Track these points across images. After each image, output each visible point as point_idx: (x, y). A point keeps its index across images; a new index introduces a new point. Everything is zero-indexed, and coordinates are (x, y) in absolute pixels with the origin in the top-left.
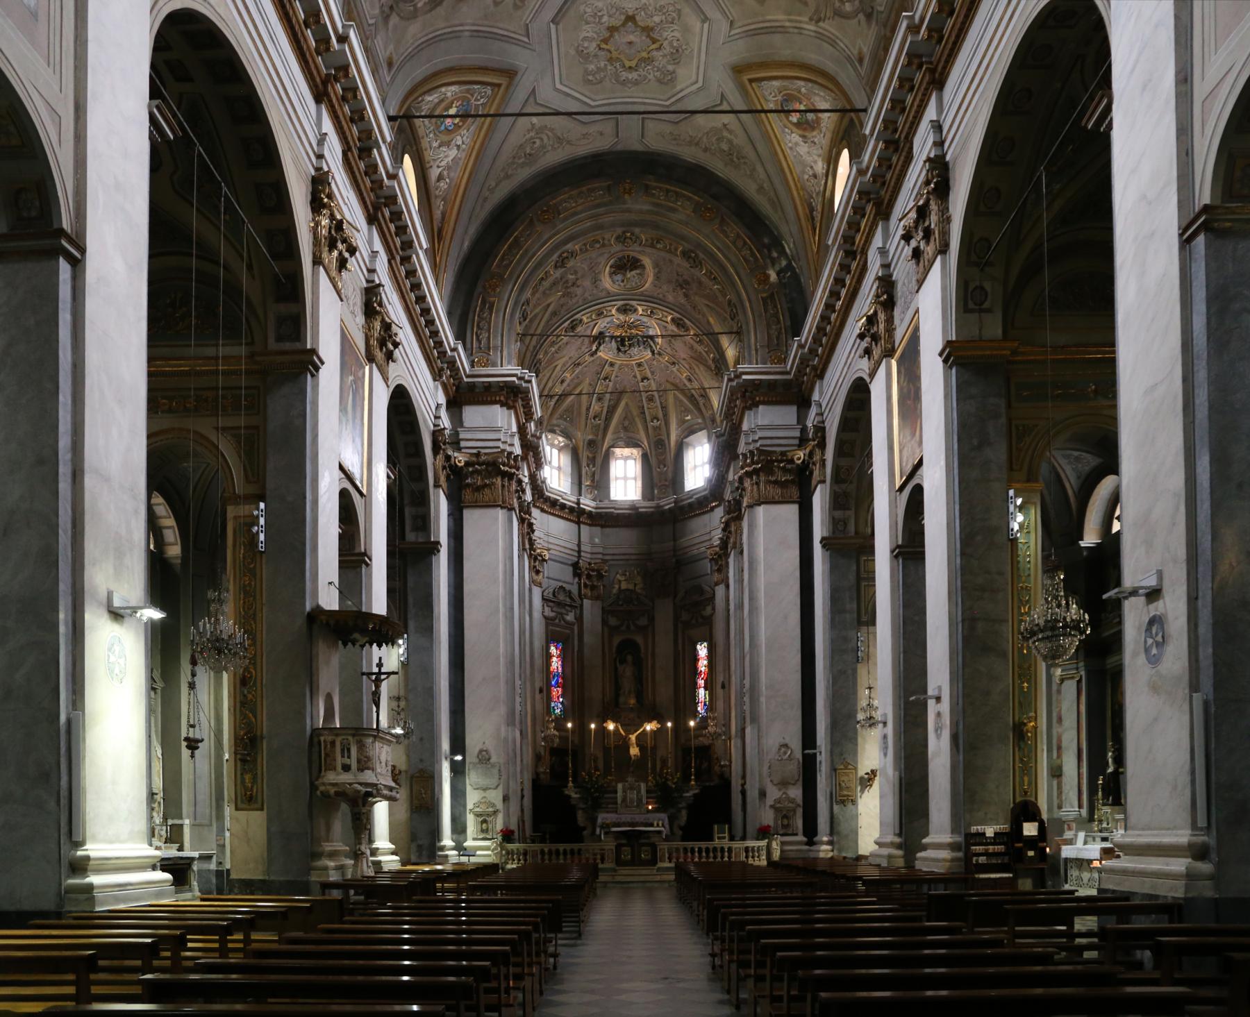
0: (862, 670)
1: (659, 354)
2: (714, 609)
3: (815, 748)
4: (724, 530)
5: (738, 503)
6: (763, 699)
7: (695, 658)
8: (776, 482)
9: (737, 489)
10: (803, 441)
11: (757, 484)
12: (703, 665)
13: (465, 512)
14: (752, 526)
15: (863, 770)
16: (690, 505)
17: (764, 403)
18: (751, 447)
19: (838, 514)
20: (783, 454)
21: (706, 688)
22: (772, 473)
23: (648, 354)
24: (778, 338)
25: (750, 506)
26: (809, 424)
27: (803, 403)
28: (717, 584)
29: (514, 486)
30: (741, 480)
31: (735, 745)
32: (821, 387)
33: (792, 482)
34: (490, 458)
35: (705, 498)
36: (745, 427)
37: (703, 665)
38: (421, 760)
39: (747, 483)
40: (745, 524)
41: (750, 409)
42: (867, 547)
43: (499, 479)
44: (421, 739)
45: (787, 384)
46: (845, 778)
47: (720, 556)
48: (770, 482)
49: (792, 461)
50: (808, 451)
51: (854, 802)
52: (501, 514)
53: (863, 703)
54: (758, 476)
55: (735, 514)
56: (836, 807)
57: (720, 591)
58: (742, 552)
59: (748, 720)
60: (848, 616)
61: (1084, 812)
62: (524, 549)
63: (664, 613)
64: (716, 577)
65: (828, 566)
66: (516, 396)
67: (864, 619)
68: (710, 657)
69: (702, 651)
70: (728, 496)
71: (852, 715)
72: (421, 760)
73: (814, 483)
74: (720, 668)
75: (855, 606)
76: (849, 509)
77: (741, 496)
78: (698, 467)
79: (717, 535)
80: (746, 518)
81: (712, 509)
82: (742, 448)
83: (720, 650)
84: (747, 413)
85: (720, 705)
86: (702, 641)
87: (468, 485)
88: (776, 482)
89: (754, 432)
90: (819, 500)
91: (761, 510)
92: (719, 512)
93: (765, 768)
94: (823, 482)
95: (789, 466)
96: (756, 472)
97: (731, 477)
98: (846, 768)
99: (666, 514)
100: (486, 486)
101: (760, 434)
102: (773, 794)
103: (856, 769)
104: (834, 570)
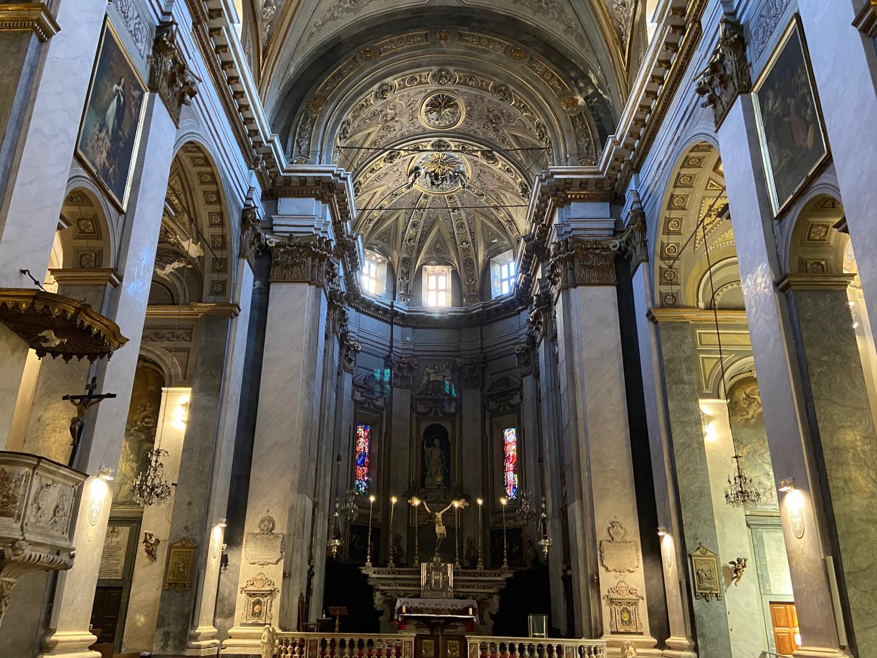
13: (272, 286)
24: (587, 149)
43: (310, 259)
45: (599, 183)
52: (308, 290)
66: (331, 191)
87: (277, 264)
100: (295, 264)
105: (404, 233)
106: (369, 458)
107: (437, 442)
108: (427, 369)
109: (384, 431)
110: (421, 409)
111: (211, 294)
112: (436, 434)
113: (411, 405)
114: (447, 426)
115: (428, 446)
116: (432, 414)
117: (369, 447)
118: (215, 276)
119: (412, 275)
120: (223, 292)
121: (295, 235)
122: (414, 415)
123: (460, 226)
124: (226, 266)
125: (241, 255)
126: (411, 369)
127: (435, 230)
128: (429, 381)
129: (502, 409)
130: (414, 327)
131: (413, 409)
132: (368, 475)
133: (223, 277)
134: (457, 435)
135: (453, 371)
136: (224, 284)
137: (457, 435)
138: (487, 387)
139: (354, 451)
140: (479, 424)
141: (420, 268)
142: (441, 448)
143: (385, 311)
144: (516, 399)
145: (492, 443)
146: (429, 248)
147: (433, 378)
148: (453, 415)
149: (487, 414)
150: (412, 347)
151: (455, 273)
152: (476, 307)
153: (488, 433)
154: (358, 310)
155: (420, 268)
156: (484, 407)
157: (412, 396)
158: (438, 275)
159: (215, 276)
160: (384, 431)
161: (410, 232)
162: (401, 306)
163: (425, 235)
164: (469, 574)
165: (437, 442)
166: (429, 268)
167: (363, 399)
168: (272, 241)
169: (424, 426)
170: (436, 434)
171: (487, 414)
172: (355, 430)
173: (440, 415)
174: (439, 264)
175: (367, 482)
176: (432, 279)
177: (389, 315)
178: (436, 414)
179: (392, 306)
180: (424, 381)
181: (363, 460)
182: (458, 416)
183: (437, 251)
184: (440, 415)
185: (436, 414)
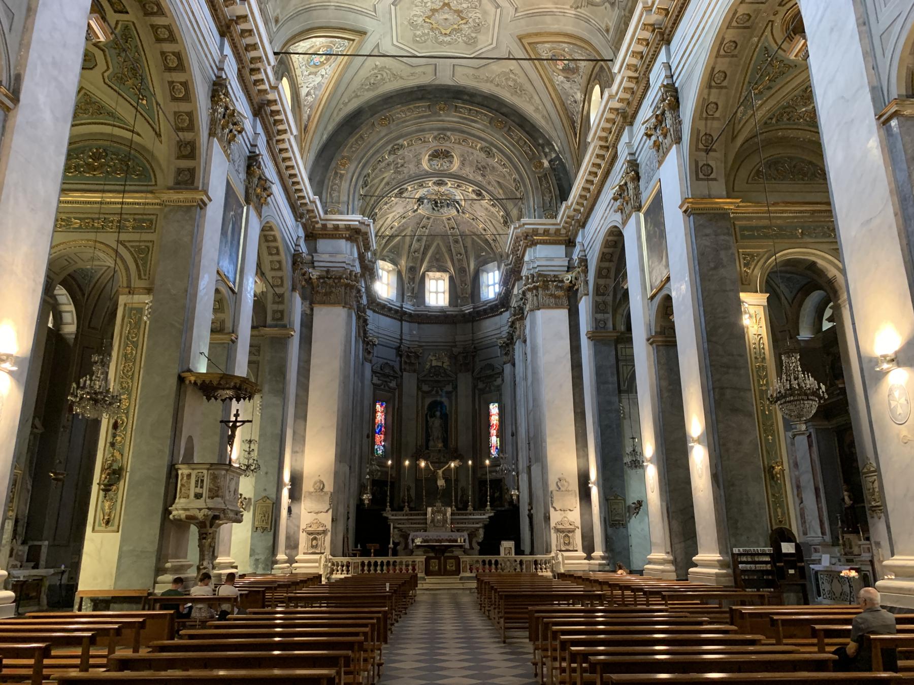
0: (626, 423)
1: (463, 213)
2: (503, 380)
4: (511, 326)
5: (521, 309)
7: (488, 415)
8: (551, 295)
9: (522, 299)
10: (570, 268)
12: (494, 419)
14: (533, 323)
16: (485, 310)
18: (532, 272)
19: (599, 316)
20: (555, 276)
21: (497, 436)
22: (548, 289)
25: (532, 310)
26: (575, 257)
27: (570, 243)
28: (505, 363)
29: (354, 292)
30: (524, 293)
31: (524, 478)
35: (496, 305)
36: (526, 258)
37: (494, 419)
38: (265, 490)
39: (529, 295)
40: (528, 322)
41: (530, 246)
42: (625, 337)
44: (267, 473)
46: (615, 506)
47: (507, 345)
49: (562, 281)
50: (574, 275)
51: (625, 526)
53: (629, 449)
55: (520, 314)
57: (508, 368)
58: (525, 341)
59: (533, 460)
60: (610, 386)
61: (828, 538)
62: (359, 336)
63: (464, 383)
64: (505, 358)
65: (592, 352)
67: (623, 388)
68: (501, 414)
69: (494, 409)
70: (514, 303)
71: (618, 458)
72: (265, 490)
73: (579, 295)
74: (508, 421)
75: (616, 379)
76: (608, 313)
77: (524, 304)
78: (491, 284)
79: (506, 329)
80: (528, 318)
81: (501, 313)
82: (524, 272)
83: (508, 408)
84: (528, 250)
85: (509, 448)
86: (494, 402)
88: (551, 295)
89: (532, 262)
90: (585, 306)
91: (540, 314)
92: (507, 315)
94: (587, 294)
96: (536, 288)
97: (515, 291)
98: (616, 499)
99: (467, 313)
101: (538, 263)
103: (624, 500)
104: (597, 353)
105: (410, 246)
109: (396, 407)
110: (425, 388)
111: (273, 319)
113: (418, 386)
114: (445, 400)
115: (431, 417)
116: (434, 392)
117: (385, 419)
118: (275, 307)
119: (417, 280)
120: (281, 319)
122: (420, 393)
124: (283, 299)
126: (417, 357)
127: (435, 244)
128: (431, 367)
130: (419, 323)
131: (419, 388)
132: (384, 441)
135: (450, 358)
136: (282, 312)
138: (477, 371)
141: (424, 274)
142: (441, 418)
143: (396, 311)
144: (499, 381)
145: (480, 415)
146: (431, 258)
147: (434, 363)
151: (451, 279)
152: (468, 309)
153: (477, 407)
154: (374, 311)
156: (475, 387)
158: (437, 279)
159: (275, 307)
160: (396, 407)
161: (415, 245)
162: (408, 307)
163: (427, 248)
164: (462, 514)
165: (438, 414)
166: (431, 274)
167: (379, 382)
168: (314, 274)
169: (428, 401)
171: (477, 391)
174: (439, 271)
175: (384, 446)
176: (433, 282)
177: (398, 314)
178: (437, 392)
179: (402, 307)
180: (427, 367)
183: (437, 260)
185: (437, 392)
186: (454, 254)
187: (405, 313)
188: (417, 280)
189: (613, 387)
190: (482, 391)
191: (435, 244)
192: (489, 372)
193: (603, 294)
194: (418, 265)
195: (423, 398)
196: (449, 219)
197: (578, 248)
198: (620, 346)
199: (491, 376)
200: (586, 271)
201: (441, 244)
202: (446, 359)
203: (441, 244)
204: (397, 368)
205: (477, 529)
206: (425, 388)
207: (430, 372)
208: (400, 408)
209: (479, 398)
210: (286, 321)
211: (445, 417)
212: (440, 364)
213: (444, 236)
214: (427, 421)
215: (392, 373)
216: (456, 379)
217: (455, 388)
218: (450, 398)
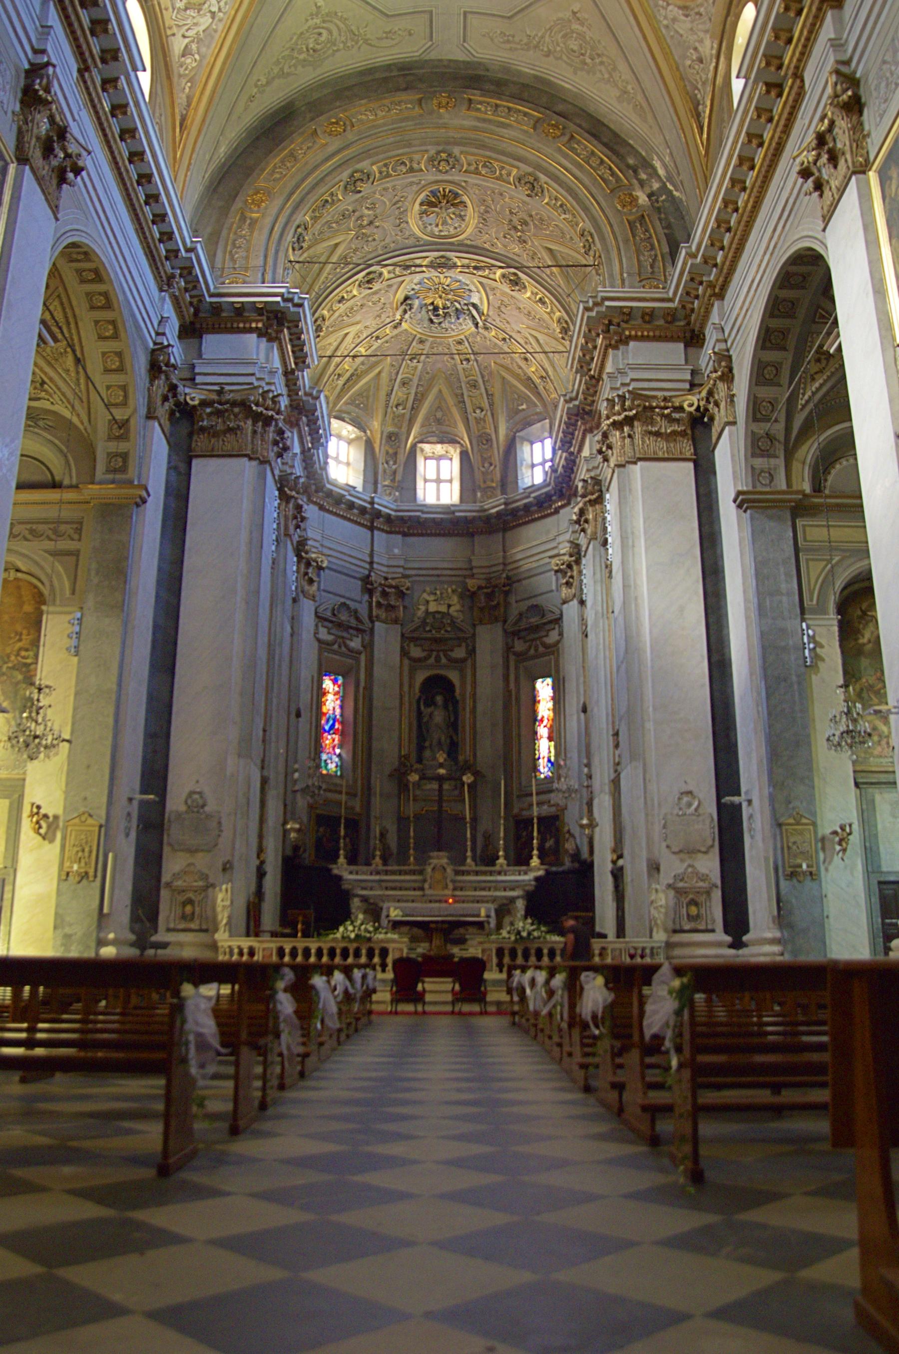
1: (486, 328)
3: (739, 795)
6: (650, 725)
8: (657, 434)
11: (630, 436)
13: (195, 462)
15: (828, 822)
17: (636, 338)
19: (759, 462)
22: (652, 422)
23: (468, 326)
24: (652, 266)
29: (271, 435)
32: (721, 308)
33: (683, 434)
34: (238, 397)
43: (250, 422)
45: (671, 316)
48: (650, 433)
49: (680, 409)
52: (248, 467)
54: (632, 426)
56: (783, 884)
66: (281, 324)
87: (203, 429)
93: (657, 828)
94: (734, 423)
95: (676, 416)
96: (629, 421)
100: (230, 430)
102: (672, 866)
105: (389, 395)
106: (342, 723)
107: (439, 699)
108: (425, 595)
109: (362, 684)
110: (416, 652)
111: (109, 471)
112: (437, 688)
113: (402, 648)
114: (454, 676)
115: (427, 705)
116: (432, 660)
117: (342, 707)
118: (113, 447)
119: (402, 458)
120: (124, 469)
121: (227, 388)
122: (406, 662)
123: (474, 385)
124: (128, 431)
125: (150, 416)
126: (401, 595)
127: (435, 391)
128: (427, 612)
129: (532, 652)
130: (405, 535)
131: (404, 653)
132: (341, 746)
133: (123, 446)
134: (469, 688)
135: (461, 597)
136: (125, 456)
137: (469, 688)
138: (512, 619)
139: (320, 714)
140: (500, 671)
142: (446, 707)
143: (363, 511)
144: (553, 637)
146: (427, 418)
147: (433, 607)
148: (463, 660)
149: (512, 658)
150: (402, 563)
151: (464, 455)
152: (494, 505)
153: (512, 685)
154: (322, 508)
155: (414, 446)
156: (508, 648)
157: (403, 635)
158: (439, 458)
159: (113, 447)
160: (362, 684)
161: (399, 393)
162: (386, 503)
163: (419, 399)
165: (439, 699)
166: (427, 447)
167: (330, 638)
168: (193, 396)
170: (437, 688)
171: (512, 658)
172: (320, 683)
173: (444, 660)
174: (441, 442)
175: (339, 756)
176: (432, 463)
177: (369, 517)
178: (438, 660)
179: (372, 503)
180: (420, 613)
181: (333, 725)
182: (469, 662)
183: (439, 422)
184: (444, 660)
185: (438, 660)
186: (470, 409)
187: (378, 514)
188: (402, 458)
189: (790, 602)
190: (522, 657)
191: (435, 391)
192: (534, 620)
193: (766, 419)
194: (404, 429)
195: (412, 672)
196: (460, 343)
197: (708, 350)
198: (799, 523)
199: (537, 628)
200: (728, 376)
201: (445, 391)
202: (455, 599)
203: (445, 391)
204: (364, 613)
205: (512, 900)
206: (416, 652)
207: (424, 623)
208: (369, 688)
209: (517, 668)
210: (132, 473)
211: (452, 702)
212: (443, 609)
213: (452, 379)
214: (419, 713)
215: (353, 623)
216: (474, 635)
217: (472, 652)
218: (462, 671)
